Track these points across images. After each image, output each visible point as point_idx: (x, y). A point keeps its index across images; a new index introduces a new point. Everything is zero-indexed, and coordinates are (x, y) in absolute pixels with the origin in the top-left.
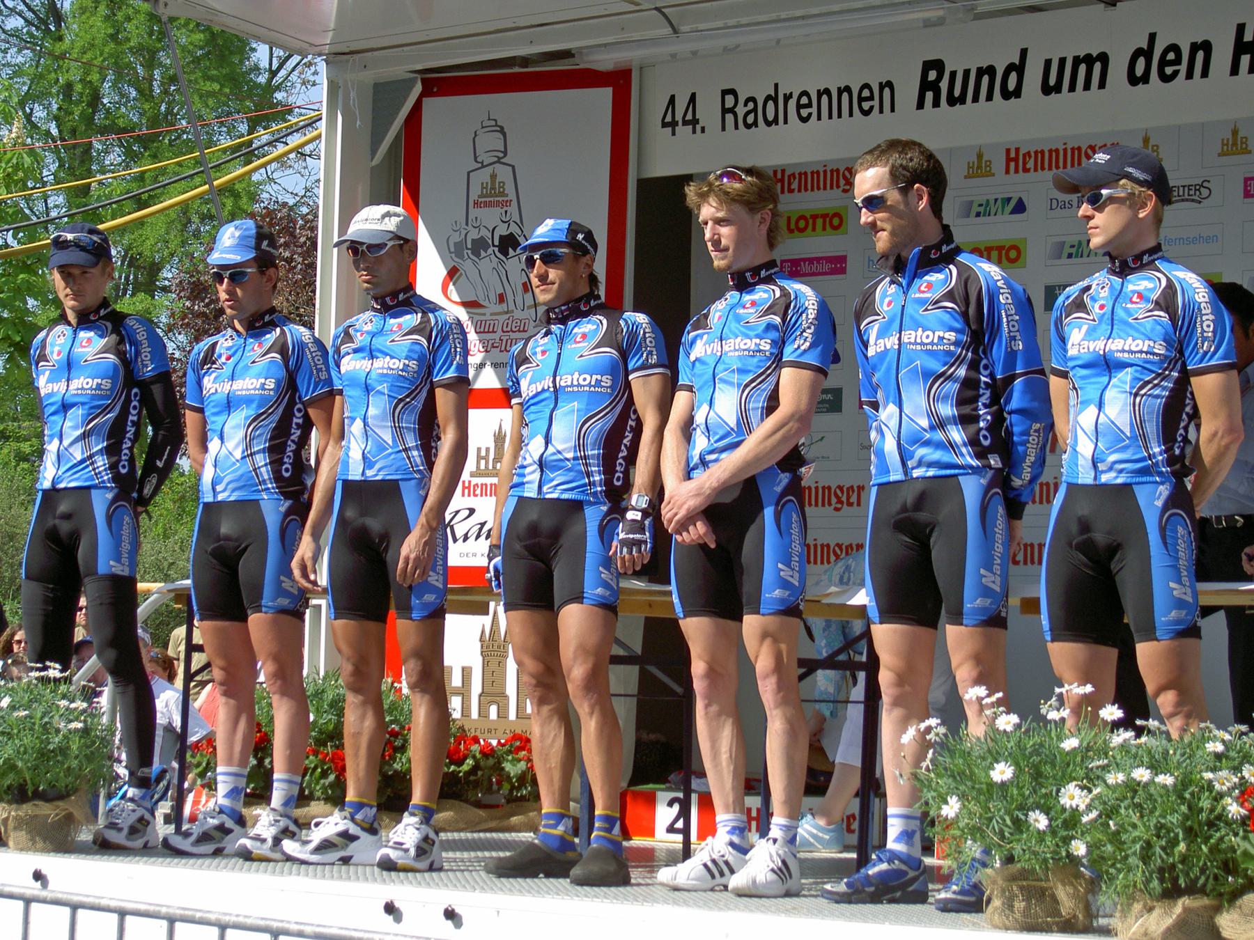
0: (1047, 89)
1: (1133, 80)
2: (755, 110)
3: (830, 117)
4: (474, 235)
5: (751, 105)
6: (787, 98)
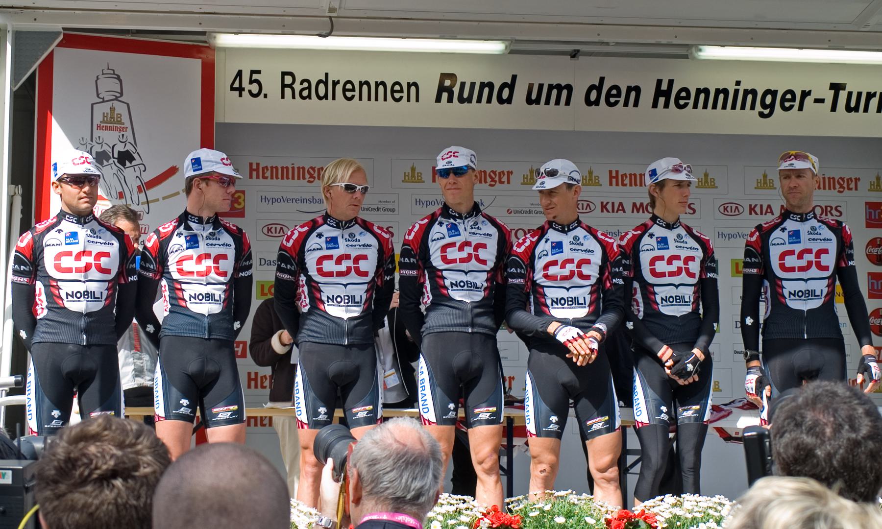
0: (529, 101)
1: (588, 102)
2: (309, 88)
3: (369, 99)
4: (97, 148)
5: (306, 85)
6: (335, 83)
